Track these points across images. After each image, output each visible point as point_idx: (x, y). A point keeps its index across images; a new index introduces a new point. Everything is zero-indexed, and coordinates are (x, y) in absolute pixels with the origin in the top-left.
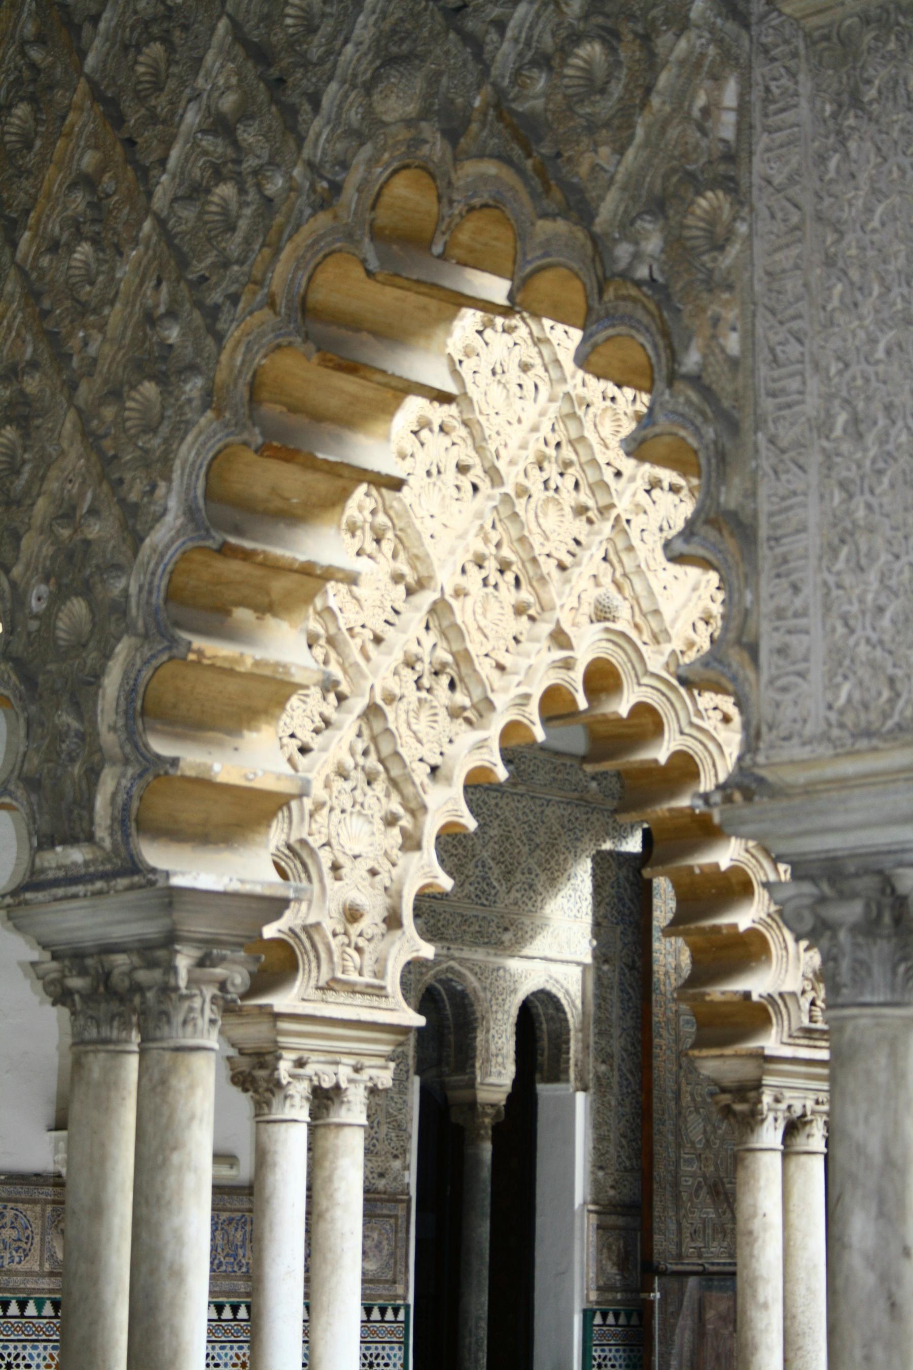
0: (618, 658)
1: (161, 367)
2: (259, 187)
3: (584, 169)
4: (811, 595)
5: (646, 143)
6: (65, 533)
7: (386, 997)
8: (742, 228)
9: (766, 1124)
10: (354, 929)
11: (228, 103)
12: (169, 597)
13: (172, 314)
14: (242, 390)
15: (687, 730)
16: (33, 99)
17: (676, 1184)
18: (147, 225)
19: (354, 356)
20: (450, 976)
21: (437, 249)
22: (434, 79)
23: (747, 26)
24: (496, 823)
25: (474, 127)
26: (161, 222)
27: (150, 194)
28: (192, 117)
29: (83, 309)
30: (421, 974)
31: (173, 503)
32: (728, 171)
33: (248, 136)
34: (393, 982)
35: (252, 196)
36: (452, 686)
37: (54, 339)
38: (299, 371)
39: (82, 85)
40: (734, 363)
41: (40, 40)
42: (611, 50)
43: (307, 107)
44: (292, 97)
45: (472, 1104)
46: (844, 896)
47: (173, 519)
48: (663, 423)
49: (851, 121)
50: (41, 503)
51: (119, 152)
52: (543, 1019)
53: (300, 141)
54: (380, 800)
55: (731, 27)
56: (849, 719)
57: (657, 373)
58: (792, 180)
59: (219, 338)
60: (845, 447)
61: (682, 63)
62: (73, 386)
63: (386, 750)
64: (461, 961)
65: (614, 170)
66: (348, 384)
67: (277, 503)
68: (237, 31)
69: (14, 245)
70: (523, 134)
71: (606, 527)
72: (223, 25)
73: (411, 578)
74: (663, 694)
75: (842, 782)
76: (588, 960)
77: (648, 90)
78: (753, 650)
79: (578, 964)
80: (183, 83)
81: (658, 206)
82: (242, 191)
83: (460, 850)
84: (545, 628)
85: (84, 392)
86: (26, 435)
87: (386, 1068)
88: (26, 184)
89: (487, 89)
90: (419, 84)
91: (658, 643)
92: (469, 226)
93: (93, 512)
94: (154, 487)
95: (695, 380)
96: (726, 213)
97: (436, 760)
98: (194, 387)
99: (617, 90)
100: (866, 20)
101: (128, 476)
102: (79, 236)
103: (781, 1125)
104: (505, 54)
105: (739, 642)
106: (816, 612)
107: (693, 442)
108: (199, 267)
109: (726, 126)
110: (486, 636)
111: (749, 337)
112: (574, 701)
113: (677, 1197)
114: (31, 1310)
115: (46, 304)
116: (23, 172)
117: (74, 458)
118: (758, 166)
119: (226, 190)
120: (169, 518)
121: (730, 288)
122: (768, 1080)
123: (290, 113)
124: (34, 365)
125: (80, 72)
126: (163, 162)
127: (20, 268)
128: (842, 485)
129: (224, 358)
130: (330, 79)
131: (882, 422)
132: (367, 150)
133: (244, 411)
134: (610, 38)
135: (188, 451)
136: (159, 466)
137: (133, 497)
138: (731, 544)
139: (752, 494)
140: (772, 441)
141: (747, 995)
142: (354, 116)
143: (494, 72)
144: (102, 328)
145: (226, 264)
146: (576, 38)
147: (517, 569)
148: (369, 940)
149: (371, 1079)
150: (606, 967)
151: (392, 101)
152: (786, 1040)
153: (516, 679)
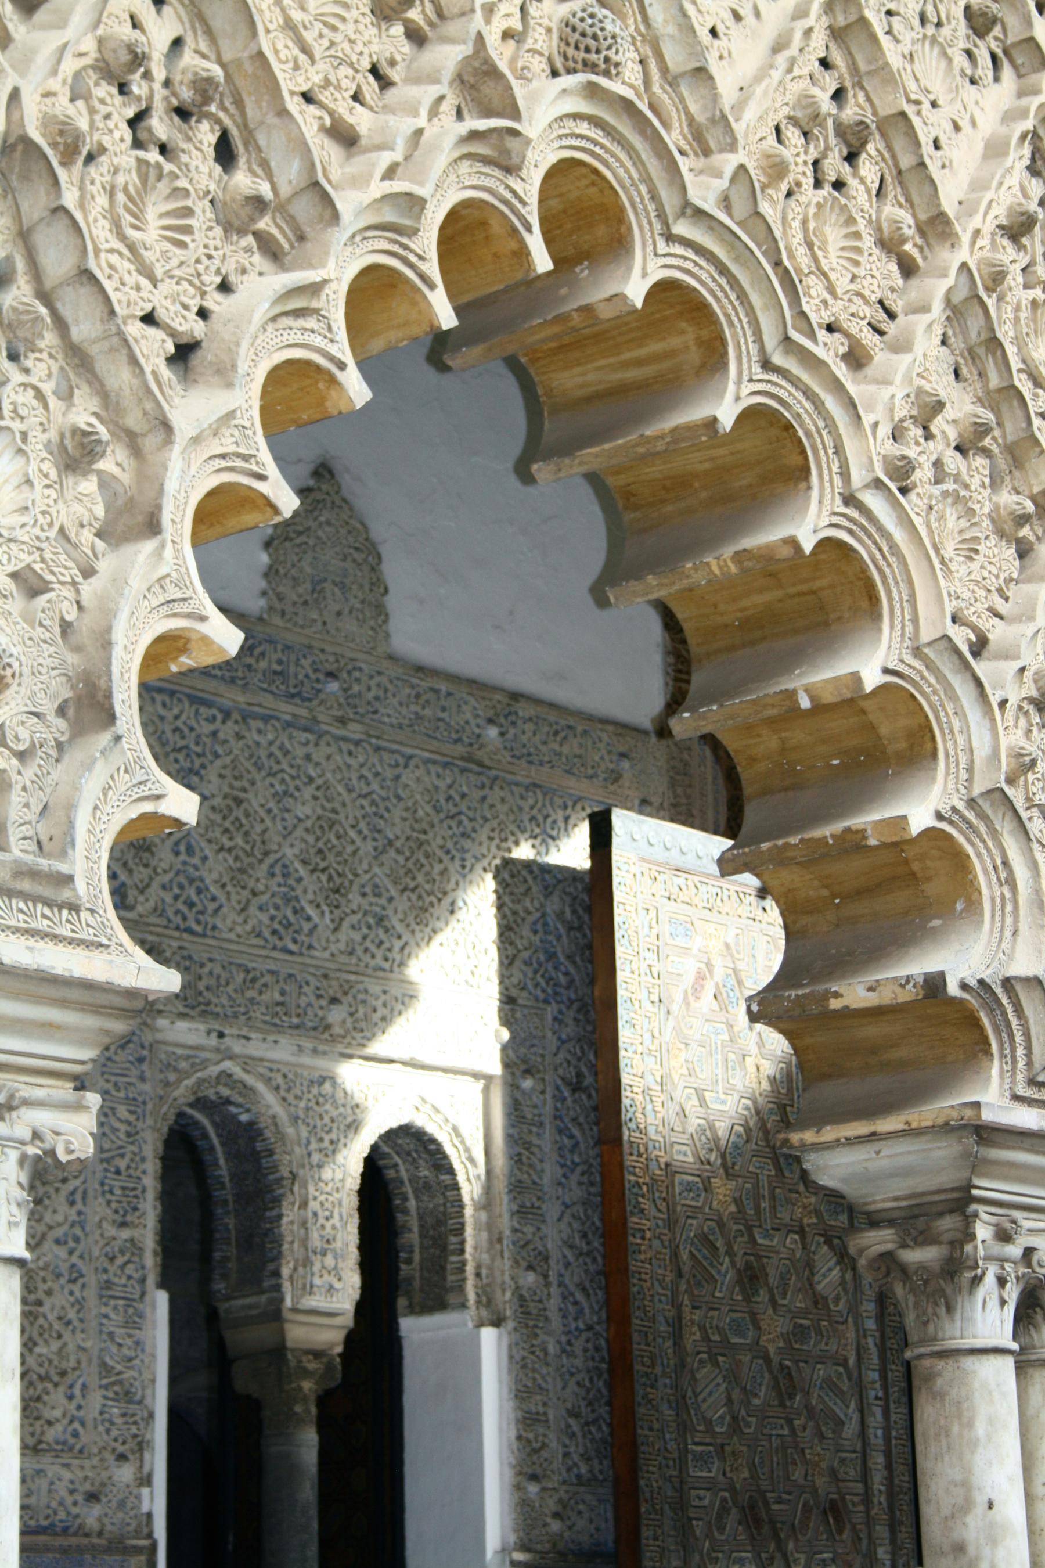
7: (74, 908)
9: (981, 1292)
15: (778, 359)
17: (681, 1505)
20: (225, 1092)
24: (308, 792)
30: (167, 1084)
34: (89, 869)
36: (225, 153)
45: (279, 1351)
52: (409, 1189)
63: (57, 263)
64: (248, 1063)
74: (723, 270)
76: (495, 1067)
79: (476, 1076)
83: (239, 840)
84: (448, 56)
87: (79, 1107)
91: (707, 152)
97: (192, 326)
103: (1013, 1293)
110: (306, 50)
112: (523, 253)
113: (684, 1530)
122: (986, 1187)
141: (935, 984)
148: (21, 756)
149: (36, 1135)
150: (528, 1083)
152: (1021, 1090)
153: (386, 159)
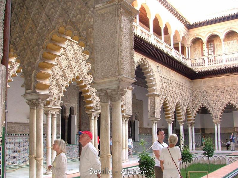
0: (79, 76)
1: (38, 45)
2: (47, 28)
3: (79, 26)
4: (99, 65)
5: (84, 24)
6: (28, 61)
8: (93, 32)
10: (55, 100)
11: (45, 20)
12: (39, 67)
13: (39, 40)
14: (46, 47)
16: (26, 20)
18: (37, 32)
19: (56, 44)
21: (64, 34)
22: (64, 18)
23: (94, 14)
25: (68, 22)
26: (38, 31)
27: (37, 29)
28: (41, 22)
29: (30, 40)
31: (39, 58)
32: (92, 27)
33: (46, 23)
34: (59, 105)
35: (47, 29)
37: (28, 43)
38: (51, 45)
39: (30, 19)
40: (92, 44)
41: (26, 14)
42: (81, 16)
43: (52, 21)
44: (51, 20)
45: (66, 117)
46: (102, 93)
47: (39, 59)
48: (86, 50)
49: (103, 22)
50: (26, 58)
51: (34, 25)
53: (51, 24)
54: (58, 88)
55: (92, 14)
56: (103, 76)
57: (86, 45)
58: (98, 27)
59: (44, 42)
60: (103, 52)
61: (88, 17)
62: (29, 47)
63: (58, 83)
65: (81, 26)
66: (56, 47)
67: (49, 58)
68: (46, 14)
69: (24, 34)
70: (73, 23)
71: (78, 64)
72: (44, 13)
73: (60, 68)
75: (102, 82)
77: (85, 19)
78: (94, 70)
80: (40, 18)
81: (86, 30)
82: (46, 28)
84: (73, 73)
85: (31, 47)
86: (25, 51)
88: (25, 28)
89: (69, 19)
90: (63, 18)
92: (68, 32)
93: (31, 59)
94: (37, 56)
95: (89, 46)
96: (92, 30)
97: (63, 84)
98: (41, 47)
99: (82, 19)
100: (105, 13)
101: (35, 55)
102: (30, 33)
104: (71, 16)
105: (93, 69)
106: (100, 67)
107: (88, 51)
108: (42, 36)
109: (92, 23)
111: (94, 42)
114: (26, 135)
115: (27, 39)
116: (24, 27)
117: (29, 53)
118: (95, 26)
119: (44, 28)
120: (39, 59)
121: (92, 37)
122: (93, 113)
123: (51, 21)
124: (26, 45)
125: (30, 17)
126: (38, 26)
127: (24, 36)
128: (103, 55)
129: (44, 44)
130: (54, 18)
131: (106, 49)
132: (58, 25)
133: (46, 49)
134: (81, 14)
135: (40, 53)
136: (38, 54)
137: (35, 57)
138: (92, 61)
139: (94, 56)
140: (96, 51)
142: (57, 22)
143: (70, 17)
144: (32, 41)
145: (44, 35)
146: (78, 15)
147: (70, 67)
151: (60, 20)
